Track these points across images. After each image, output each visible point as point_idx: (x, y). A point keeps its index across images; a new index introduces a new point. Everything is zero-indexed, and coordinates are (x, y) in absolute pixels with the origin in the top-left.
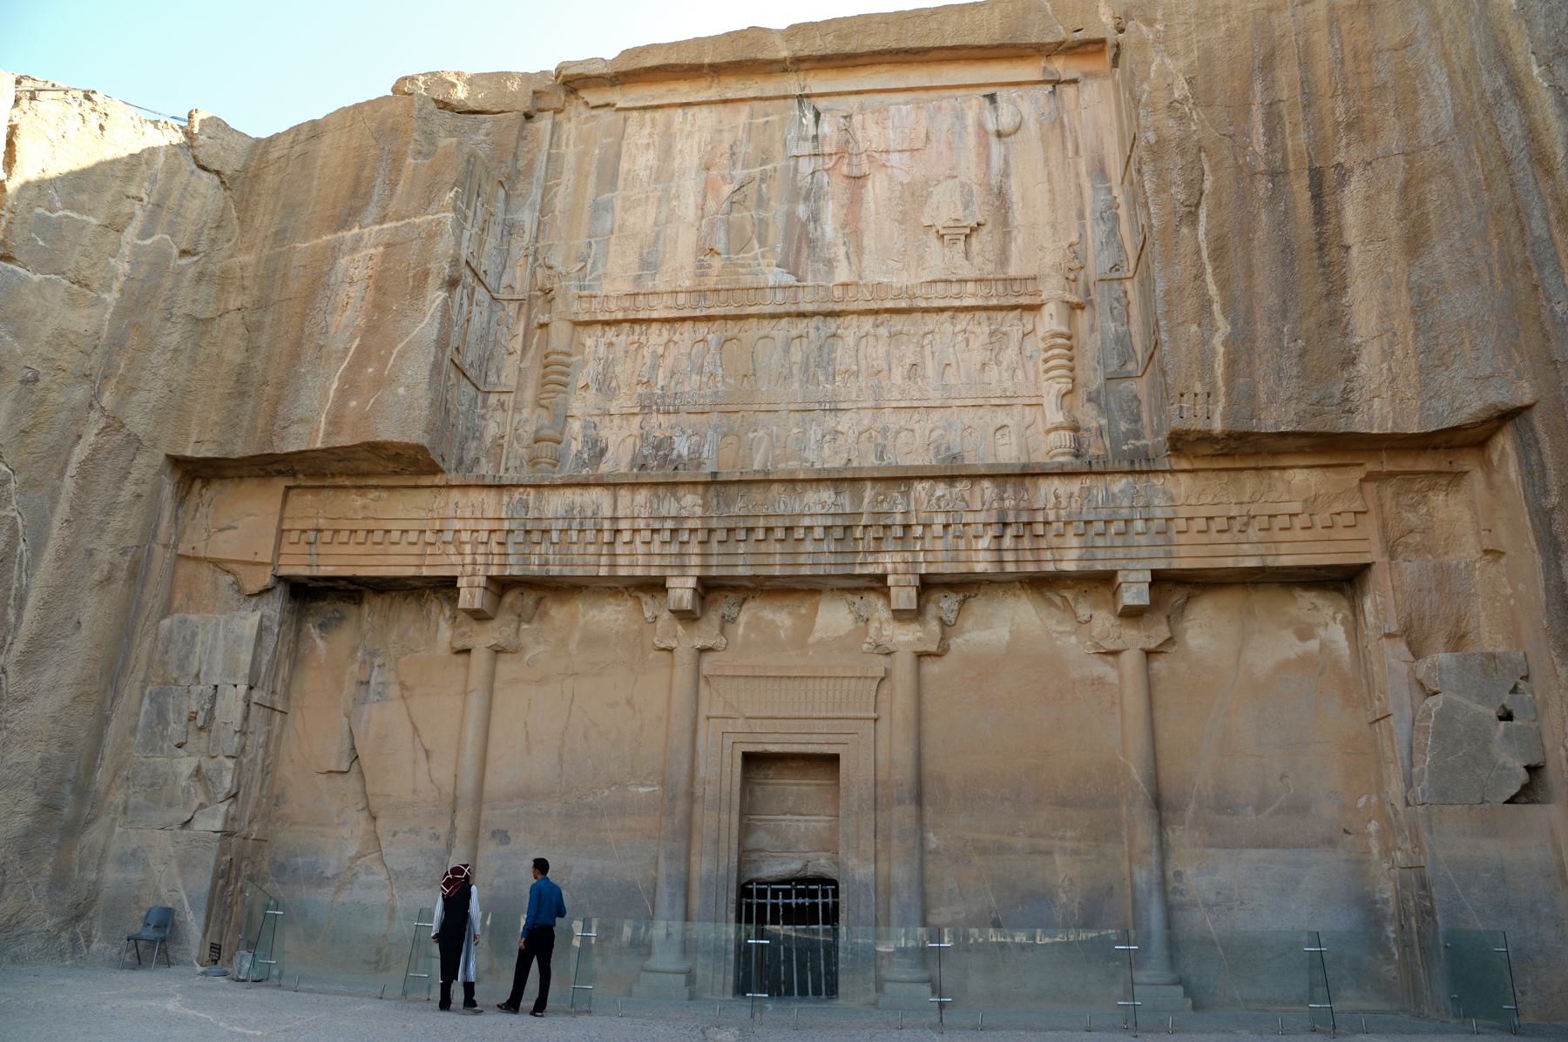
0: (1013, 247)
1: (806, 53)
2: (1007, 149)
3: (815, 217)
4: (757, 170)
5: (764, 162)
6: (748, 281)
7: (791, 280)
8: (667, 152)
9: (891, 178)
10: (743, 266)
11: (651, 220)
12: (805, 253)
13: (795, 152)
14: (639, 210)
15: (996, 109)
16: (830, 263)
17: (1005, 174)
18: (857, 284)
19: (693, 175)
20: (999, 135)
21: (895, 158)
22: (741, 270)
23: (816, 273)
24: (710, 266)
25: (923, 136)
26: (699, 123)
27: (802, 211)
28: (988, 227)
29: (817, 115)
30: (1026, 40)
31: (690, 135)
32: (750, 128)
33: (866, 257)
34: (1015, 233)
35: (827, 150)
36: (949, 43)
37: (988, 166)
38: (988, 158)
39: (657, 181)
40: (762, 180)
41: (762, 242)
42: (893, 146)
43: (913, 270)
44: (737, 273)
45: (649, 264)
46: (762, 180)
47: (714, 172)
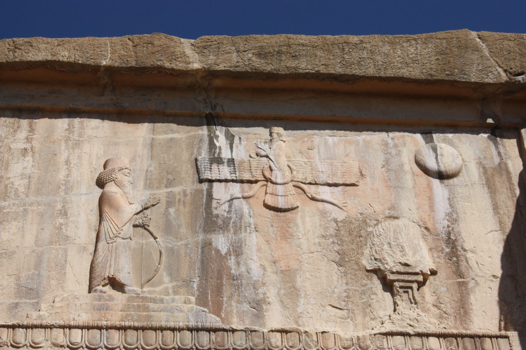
0: (472, 299)
1: (221, 67)
2: (450, 191)
3: (237, 250)
4: (162, 193)
5: (170, 184)
6: (162, 319)
7: (213, 320)
8: (49, 161)
9: (323, 214)
10: (154, 301)
11: (29, 240)
12: (227, 291)
13: (207, 175)
14: (13, 226)
15: (435, 150)
16: (258, 306)
17: (453, 218)
18: (299, 333)
19: (84, 190)
20: (442, 176)
21: (325, 193)
22: (152, 305)
23: (241, 315)
24: (111, 299)
25: (356, 170)
26: (89, 132)
27: (221, 242)
28: (442, 274)
29: (230, 138)
30: (463, 78)
31: (77, 144)
32: (152, 145)
33: (302, 301)
34: (471, 284)
35: (247, 176)
36: (382, 74)
37: (432, 207)
38: (431, 200)
39: (38, 192)
40: (169, 204)
41: (173, 274)
42: (323, 178)
43: (359, 319)
44: (147, 309)
45: (30, 292)
46: (169, 204)
47: (111, 188)
